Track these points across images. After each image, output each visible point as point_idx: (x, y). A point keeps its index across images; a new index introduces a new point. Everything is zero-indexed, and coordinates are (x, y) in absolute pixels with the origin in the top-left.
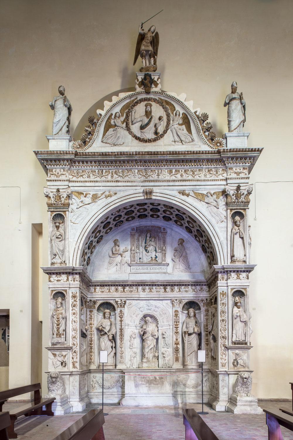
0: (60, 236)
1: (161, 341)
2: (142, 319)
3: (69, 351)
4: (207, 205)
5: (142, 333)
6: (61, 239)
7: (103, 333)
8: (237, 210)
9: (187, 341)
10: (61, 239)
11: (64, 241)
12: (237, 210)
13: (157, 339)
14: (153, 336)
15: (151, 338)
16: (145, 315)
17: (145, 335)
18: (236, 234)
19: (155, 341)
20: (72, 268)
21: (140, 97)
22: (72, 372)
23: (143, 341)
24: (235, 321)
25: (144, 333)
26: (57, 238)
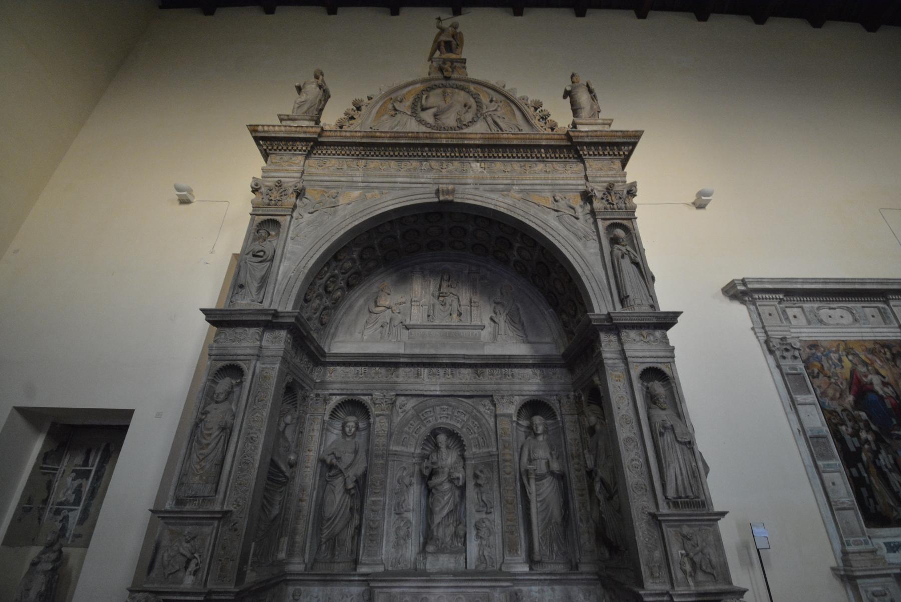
0: (261, 254)
1: (471, 492)
2: (428, 440)
3: (216, 523)
4: (556, 213)
5: (426, 473)
6: (260, 259)
7: (333, 472)
8: (615, 221)
9: (534, 495)
10: (260, 259)
11: (268, 264)
12: (615, 221)
13: (463, 489)
14: (451, 480)
15: (447, 486)
16: (435, 429)
17: (433, 478)
18: (623, 257)
19: (457, 493)
20: (273, 312)
21: (437, 83)
22: (210, 593)
23: (429, 491)
24: (660, 441)
25: (433, 473)
26: (254, 256)
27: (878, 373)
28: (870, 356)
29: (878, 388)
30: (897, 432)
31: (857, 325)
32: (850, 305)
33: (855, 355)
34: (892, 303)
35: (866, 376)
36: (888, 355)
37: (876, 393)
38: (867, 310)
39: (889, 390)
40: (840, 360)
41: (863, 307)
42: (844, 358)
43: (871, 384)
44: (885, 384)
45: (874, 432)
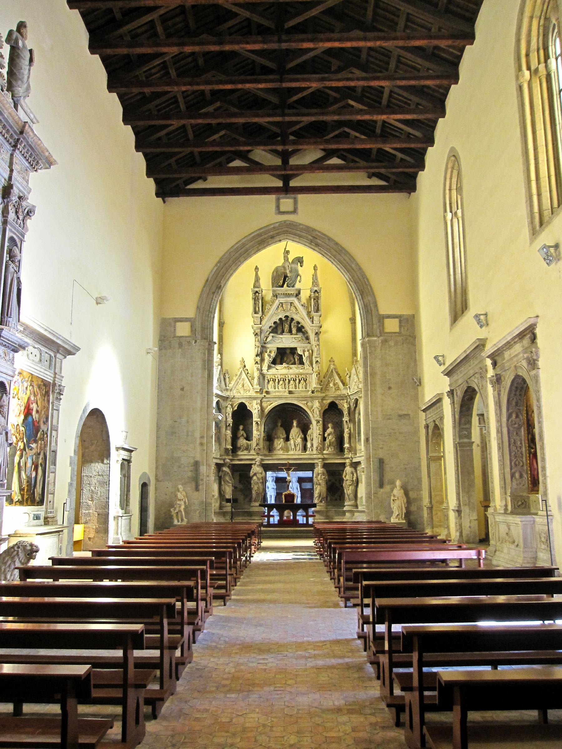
27: (37, 404)
28: (38, 390)
29: (34, 413)
30: (31, 445)
31: (40, 365)
32: (43, 349)
33: (33, 386)
34: (58, 356)
35: (32, 404)
36: (44, 392)
37: (32, 416)
38: (46, 354)
39: (37, 416)
40: (27, 388)
41: (46, 353)
42: (29, 387)
43: (32, 410)
44: (37, 411)
45: (24, 443)
